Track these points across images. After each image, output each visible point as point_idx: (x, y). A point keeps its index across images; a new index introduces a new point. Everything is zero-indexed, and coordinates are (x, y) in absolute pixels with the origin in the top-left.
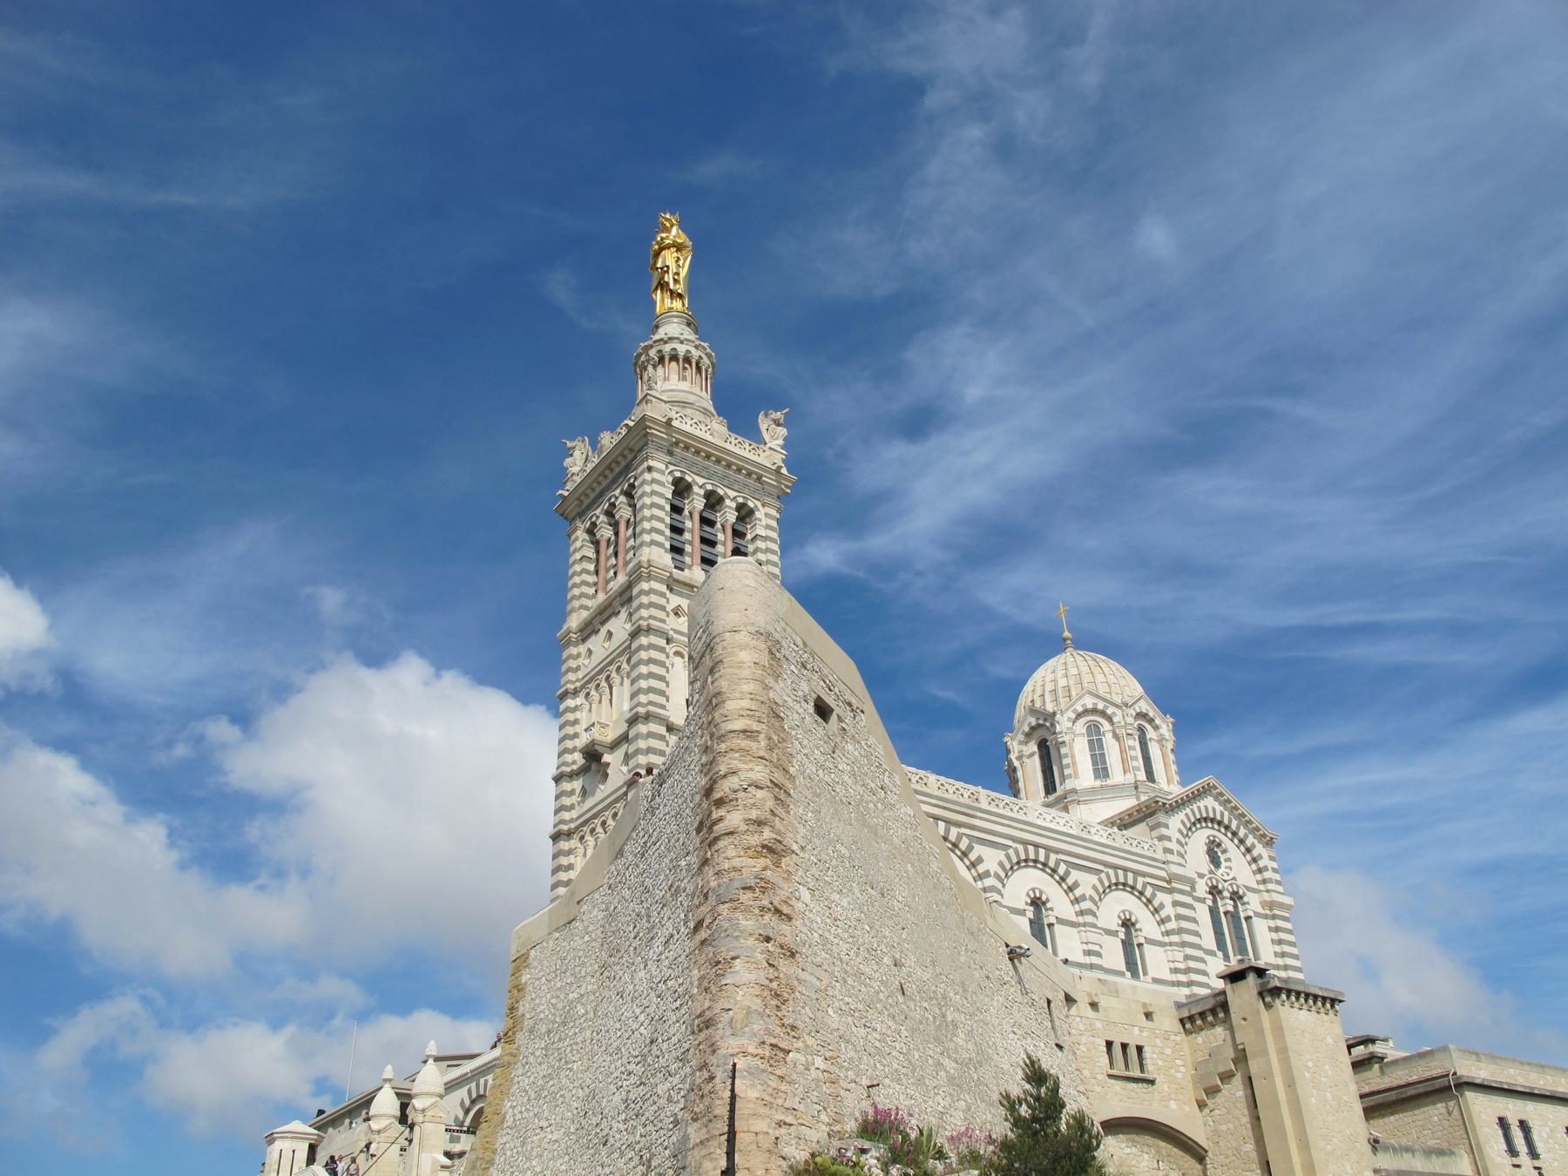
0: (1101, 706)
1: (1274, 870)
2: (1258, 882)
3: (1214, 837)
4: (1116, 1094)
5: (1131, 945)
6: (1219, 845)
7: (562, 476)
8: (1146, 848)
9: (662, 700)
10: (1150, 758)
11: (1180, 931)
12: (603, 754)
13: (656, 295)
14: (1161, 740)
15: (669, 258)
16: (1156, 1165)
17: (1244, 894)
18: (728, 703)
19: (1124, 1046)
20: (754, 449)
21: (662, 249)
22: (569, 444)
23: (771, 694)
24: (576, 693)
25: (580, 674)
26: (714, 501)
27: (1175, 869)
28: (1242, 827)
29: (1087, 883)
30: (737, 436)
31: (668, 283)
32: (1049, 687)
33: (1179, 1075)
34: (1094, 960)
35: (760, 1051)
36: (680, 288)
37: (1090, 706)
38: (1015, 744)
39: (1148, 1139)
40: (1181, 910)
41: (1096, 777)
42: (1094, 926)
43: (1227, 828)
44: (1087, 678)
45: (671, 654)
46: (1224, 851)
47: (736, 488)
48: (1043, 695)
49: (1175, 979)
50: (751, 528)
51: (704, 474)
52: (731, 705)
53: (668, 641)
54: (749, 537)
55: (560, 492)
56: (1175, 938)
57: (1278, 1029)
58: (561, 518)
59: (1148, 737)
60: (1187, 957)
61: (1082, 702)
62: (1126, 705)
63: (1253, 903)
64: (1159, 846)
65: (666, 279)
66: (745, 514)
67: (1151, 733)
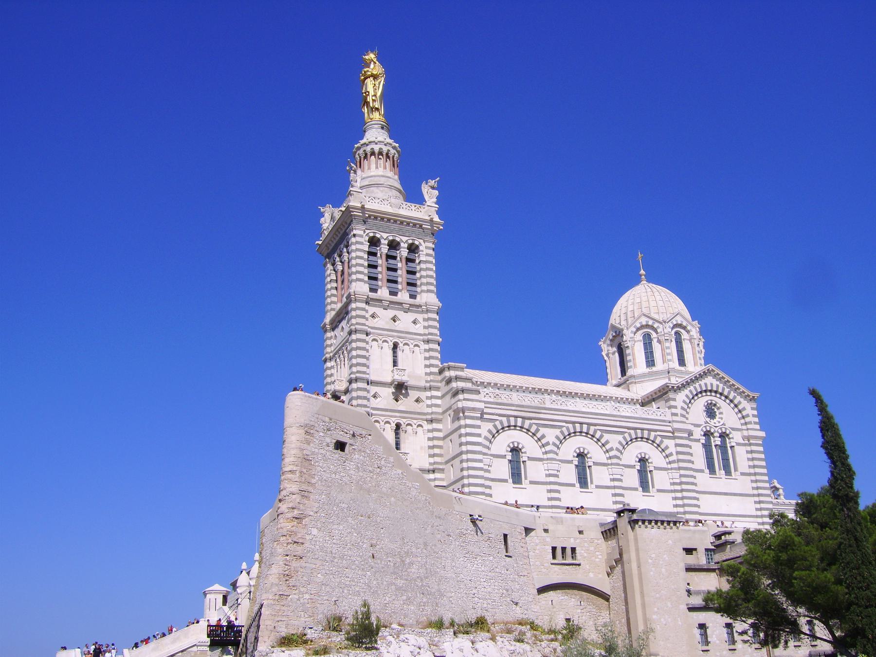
0: (650, 323)
1: (754, 416)
2: (742, 424)
3: (711, 400)
4: (555, 572)
5: (646, 471)
6: (715, 405)
8: (659, 415)
9: (364, 369)
10: (683, 351)
11: (679, 461)
13: (364, 109)
16: (579, 604)
17: (730, 433)
18: (286, 459)
19: (564, 549)
23: (305, 452)
24: (330, 359)
25: (332, 348)
26: (394, 245)
27: (676, 425)
28: (732, 392)
29: (614, 441)
31: (369, 102)
32: (624, 311)
33: (597, 560)
34: (617, 483)
35: (274, 598)
36: (377, 105)
37: (644, 323)
38: (605, 346)
39: (576, 592)
40: (680, 449)
42: (618, 464)
43: (721, 394)
44: (644, 304)
45: (370, 341)
46: (718, 408)
47: (407, 235)
49: (673, 489)
51: (387, 231)
52: (287, 460)
53: (367, 334)
54: (417, 261)
55: (317, 242)
56: (675, 465)
57: (636, 540)
58: (320, 255)
59: (683, 338)
60: (681, 476)
61: (639, 321)
62: (665, 322)
63: (736, 437)
64: (668, 412)
65: (368, 100)
66: (413, 249)
67: (684, 335)
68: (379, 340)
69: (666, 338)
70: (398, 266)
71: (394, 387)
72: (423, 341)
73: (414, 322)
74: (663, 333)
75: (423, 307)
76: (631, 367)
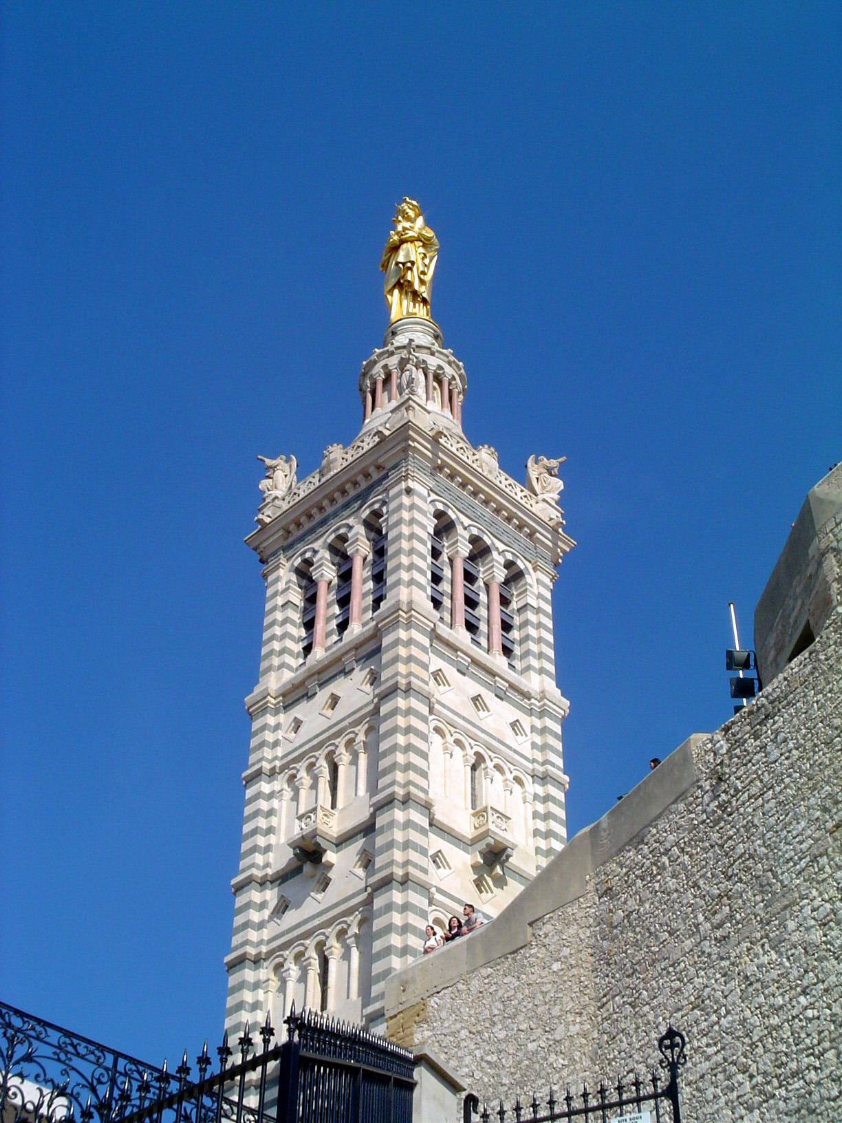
7: (259, 500)
12: (325, 851)
13: (392, 295)
15: (410, 252)
20: (525, 496)
21: (402, 242)
22: (269, 462)
25: (280, 752)
26: (480, 551)
30: (508, 477)
36: (424, 291)
50: (518, 595)
65: (409, 278)
66: (515, 576)
68: (448, 735)
70: (481, 598)
71: (480, 852)
72: (532, 777)
73: (515, 725)
75: (533, 701)
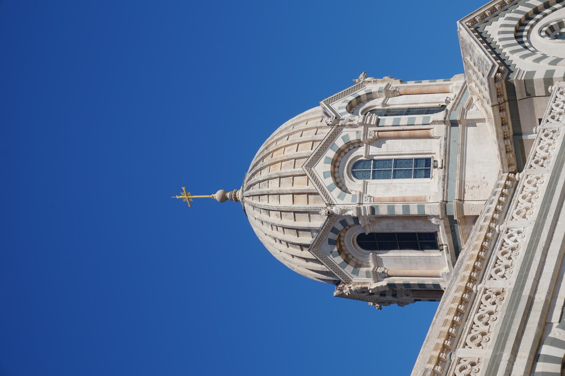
0: (331, 154)
14: (390, 93)
37: (328, 168)
38: (355, 279)
41: (427, 175)
48: (287, 243)
59: (380, 107)
67: (377, 103)
69: (374, 122)
74: (361, 129)
76: (421, 208)
